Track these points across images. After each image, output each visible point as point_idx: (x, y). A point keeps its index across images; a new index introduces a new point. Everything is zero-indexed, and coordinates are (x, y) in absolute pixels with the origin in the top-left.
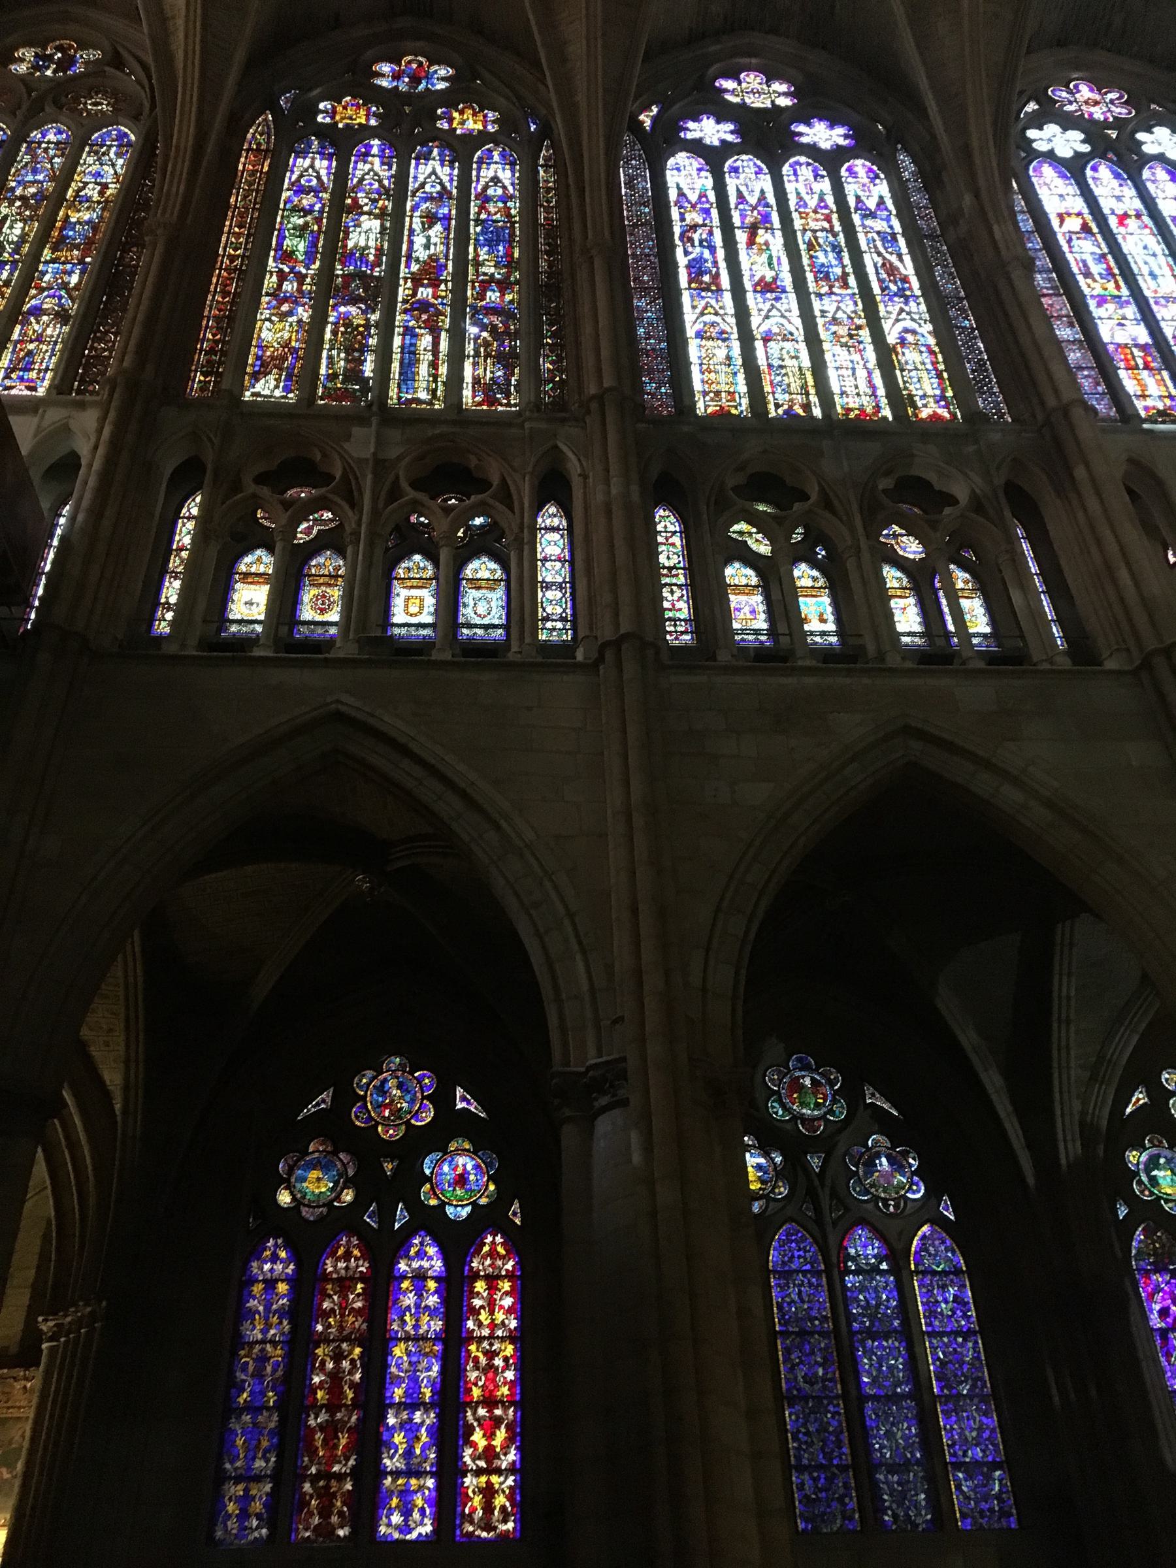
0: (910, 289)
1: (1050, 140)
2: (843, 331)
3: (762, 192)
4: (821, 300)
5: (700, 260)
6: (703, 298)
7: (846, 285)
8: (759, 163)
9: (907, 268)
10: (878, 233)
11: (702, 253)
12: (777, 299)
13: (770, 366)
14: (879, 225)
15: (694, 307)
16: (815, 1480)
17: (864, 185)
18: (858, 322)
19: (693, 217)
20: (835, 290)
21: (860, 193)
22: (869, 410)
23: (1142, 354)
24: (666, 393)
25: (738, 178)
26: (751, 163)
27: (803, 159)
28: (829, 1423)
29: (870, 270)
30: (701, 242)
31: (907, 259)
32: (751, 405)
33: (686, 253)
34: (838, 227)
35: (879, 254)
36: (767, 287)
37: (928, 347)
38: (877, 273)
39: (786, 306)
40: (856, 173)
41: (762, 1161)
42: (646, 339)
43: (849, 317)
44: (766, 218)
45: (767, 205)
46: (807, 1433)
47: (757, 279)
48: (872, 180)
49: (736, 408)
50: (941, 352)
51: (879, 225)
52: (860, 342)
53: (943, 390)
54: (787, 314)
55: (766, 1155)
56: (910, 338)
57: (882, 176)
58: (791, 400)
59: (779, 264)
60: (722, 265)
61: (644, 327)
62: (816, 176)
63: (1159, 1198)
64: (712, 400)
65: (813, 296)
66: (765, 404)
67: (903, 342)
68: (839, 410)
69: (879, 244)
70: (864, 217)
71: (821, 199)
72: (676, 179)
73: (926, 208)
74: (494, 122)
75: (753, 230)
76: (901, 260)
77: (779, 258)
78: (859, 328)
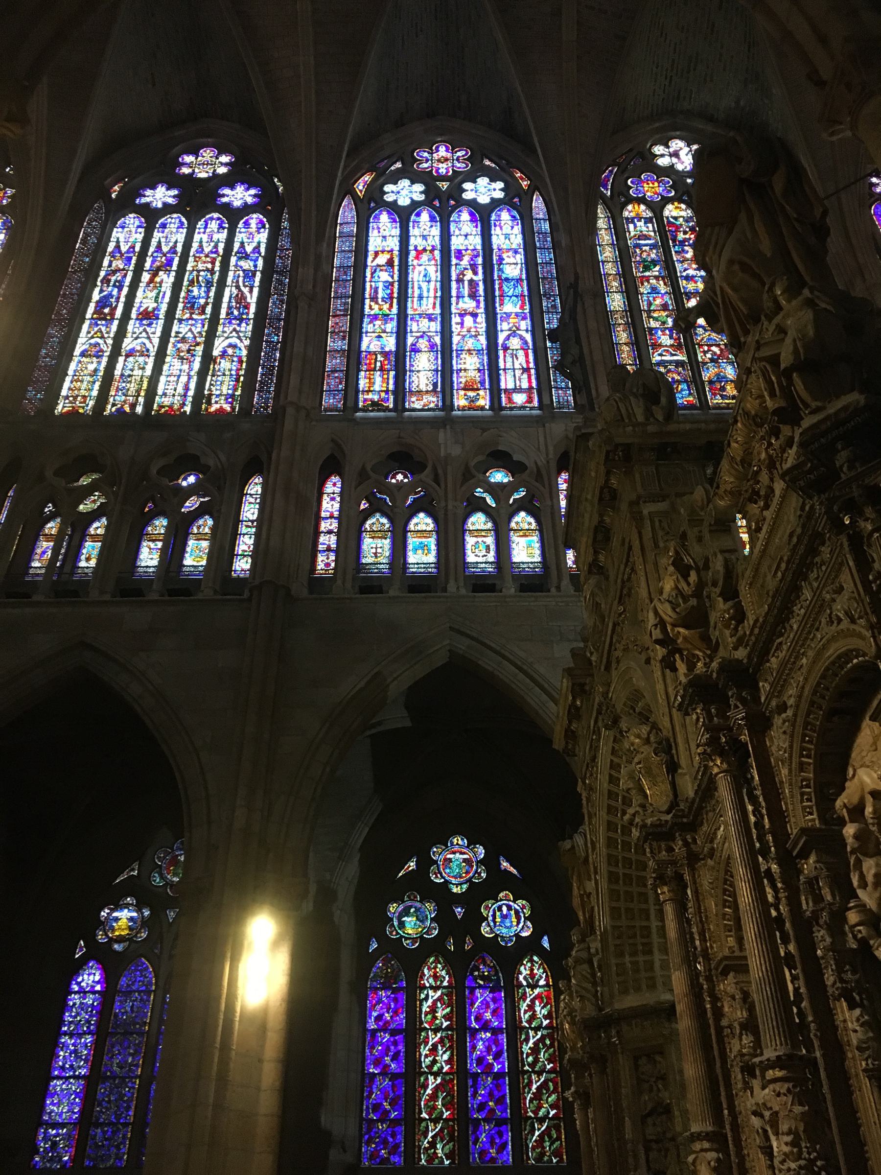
0: (248, 314)
1: (399, 192)
2: (184, 347)
3: (176, 242)
4: (181, 323)
5: (110, 295)
6: (97, 325)
7: (203, 312)
8: (184, 220)
9: (252, 299)
10: (244, 271)
11: (112, 291)
12: (149, 325)
13: (122, 375)
14: (247, 265)
15: (89, 332)
16: (104, 1133)
17: (251, 234)
18: (198, 340)
19: (119, 264)
20: (194, 316)
21: (245, 240)
22: (176, 407)
23: (382, 359)
24: (40, 399)
25: (163, 232)
26: (178, 220)
27: (216, 215)
28: (125, 1095)
29: (226, 299)
30: (116, 281)
31: (256, 291)
32: (94, 407)
33: (101, 291)
34: (217, 268)
35: (238, 287)
36: (148, 316)
37: (240, 358)
38: (230, 302)
39: (153, 330)
40: (249, 224)
41: (135, 914)
42: (45, 358)
43: (195, 337)
44: (169, 262)
45: (175, 252)
46: (109, 1102)
47: (142, 309)
48: (258, 229)
49: (83, 408)
50: (247, 362)
51: (247, 265)
52: (193, 356)
53: (235, 389)
54: (151, 336)
55: (139, 910)
56: (230, 351)
57: (267, 226)
58: (125, 401)
59: (163, 297)
60: (122, 299)
61: (47, 349)
62: (221, 227)
63: (402, 937)
64: (70, 402)
65: (176, 321)
66: (106, 402)
67: (224, 354)
68: (155, 407)
69: (241, 279)
70: (240, 259)
71: (216, 246)
72: (119, 235)
73: (287, 250)
74: (8, 197)
75: (155, 273)
76: (251, 291)
77: (165, 293)
78: (198, 344)
